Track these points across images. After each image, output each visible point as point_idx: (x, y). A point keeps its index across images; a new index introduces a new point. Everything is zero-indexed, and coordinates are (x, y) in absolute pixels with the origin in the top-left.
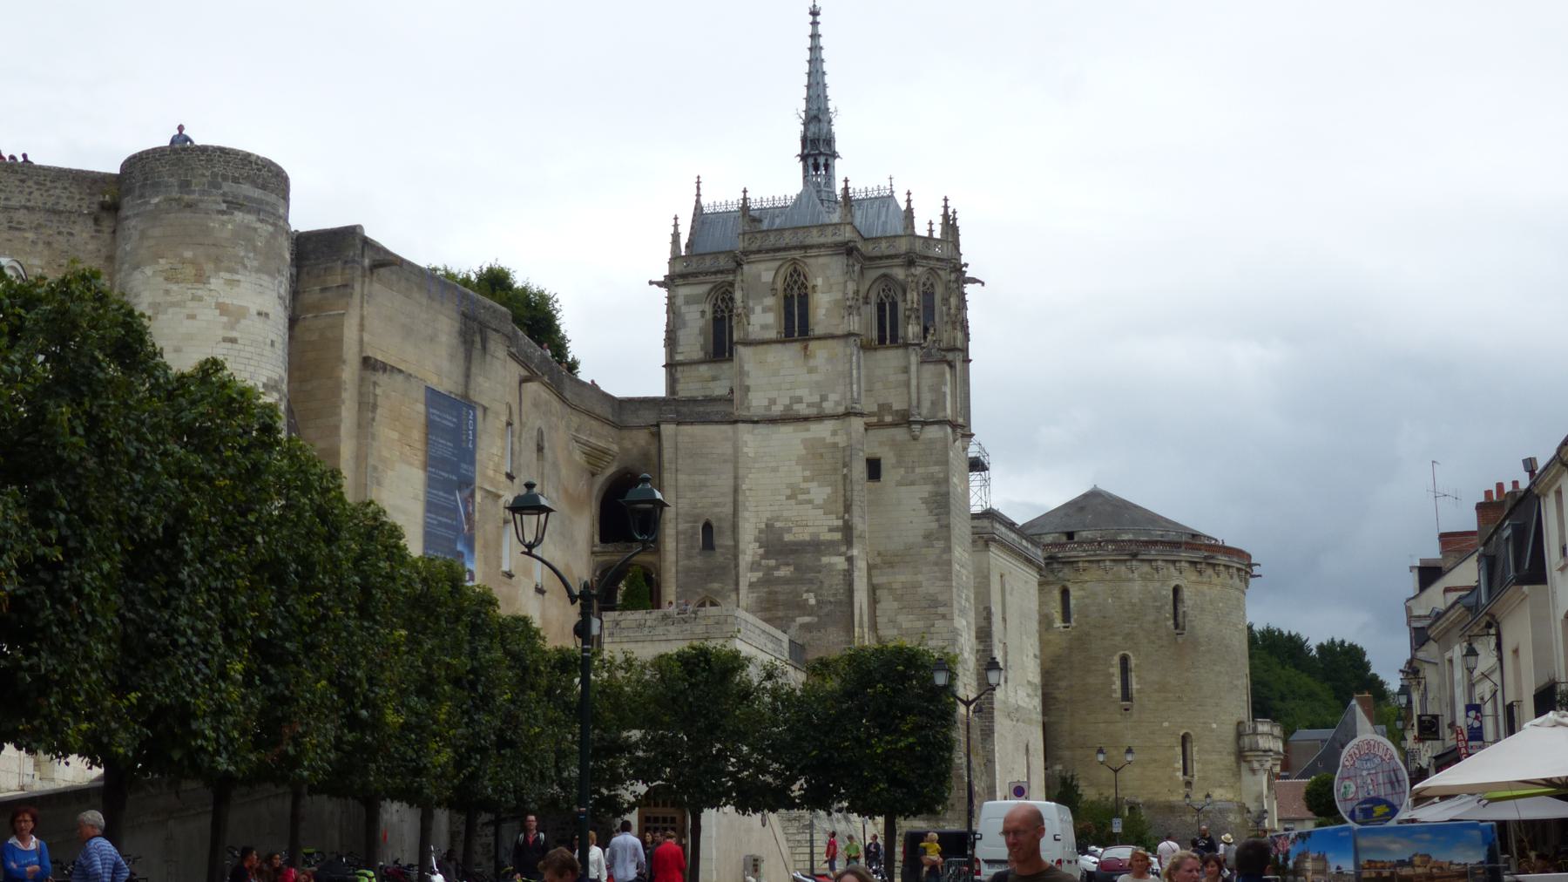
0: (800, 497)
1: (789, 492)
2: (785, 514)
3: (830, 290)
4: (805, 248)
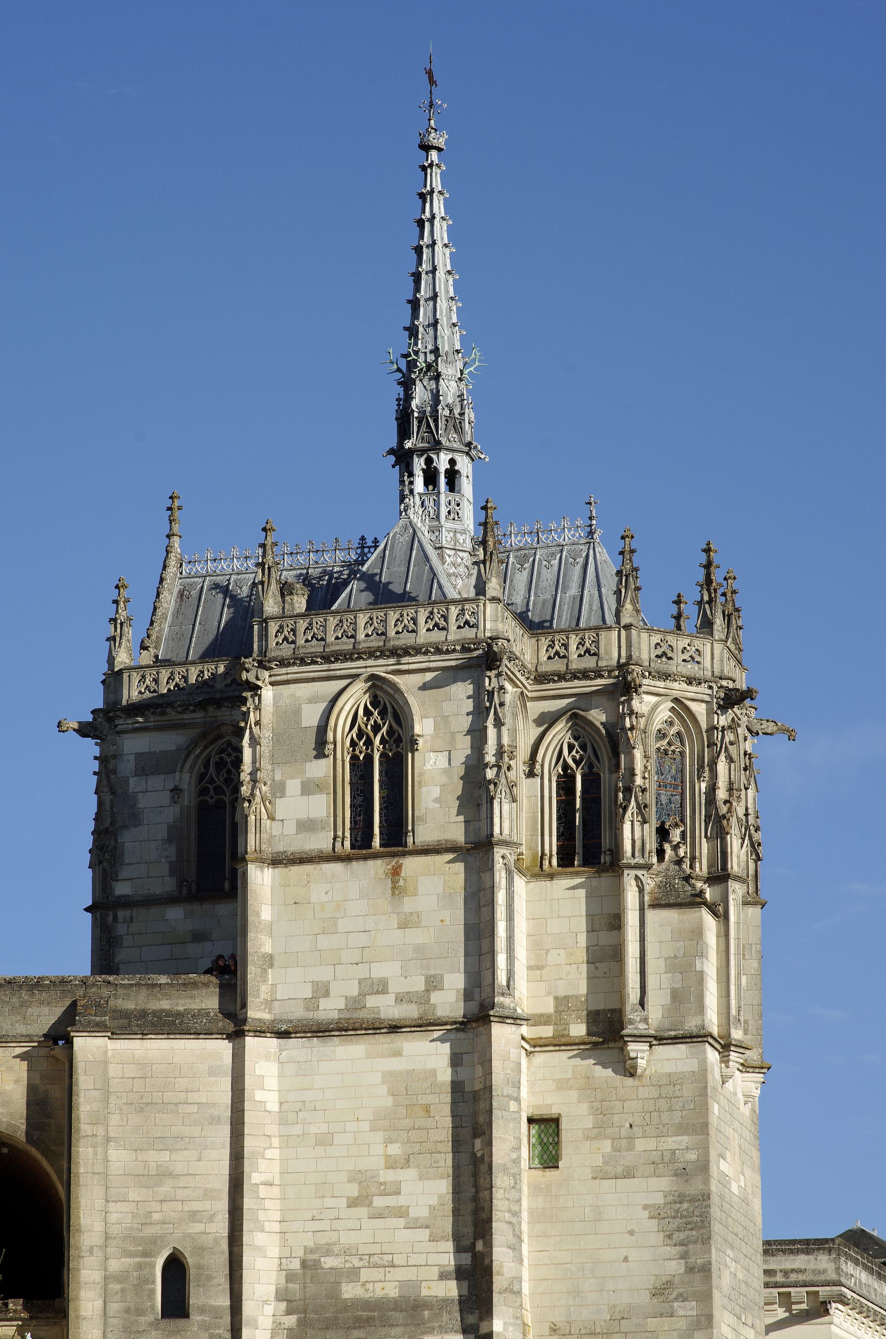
0: (379, 1202)
1: (353, 1190)
2: (347, 1239)
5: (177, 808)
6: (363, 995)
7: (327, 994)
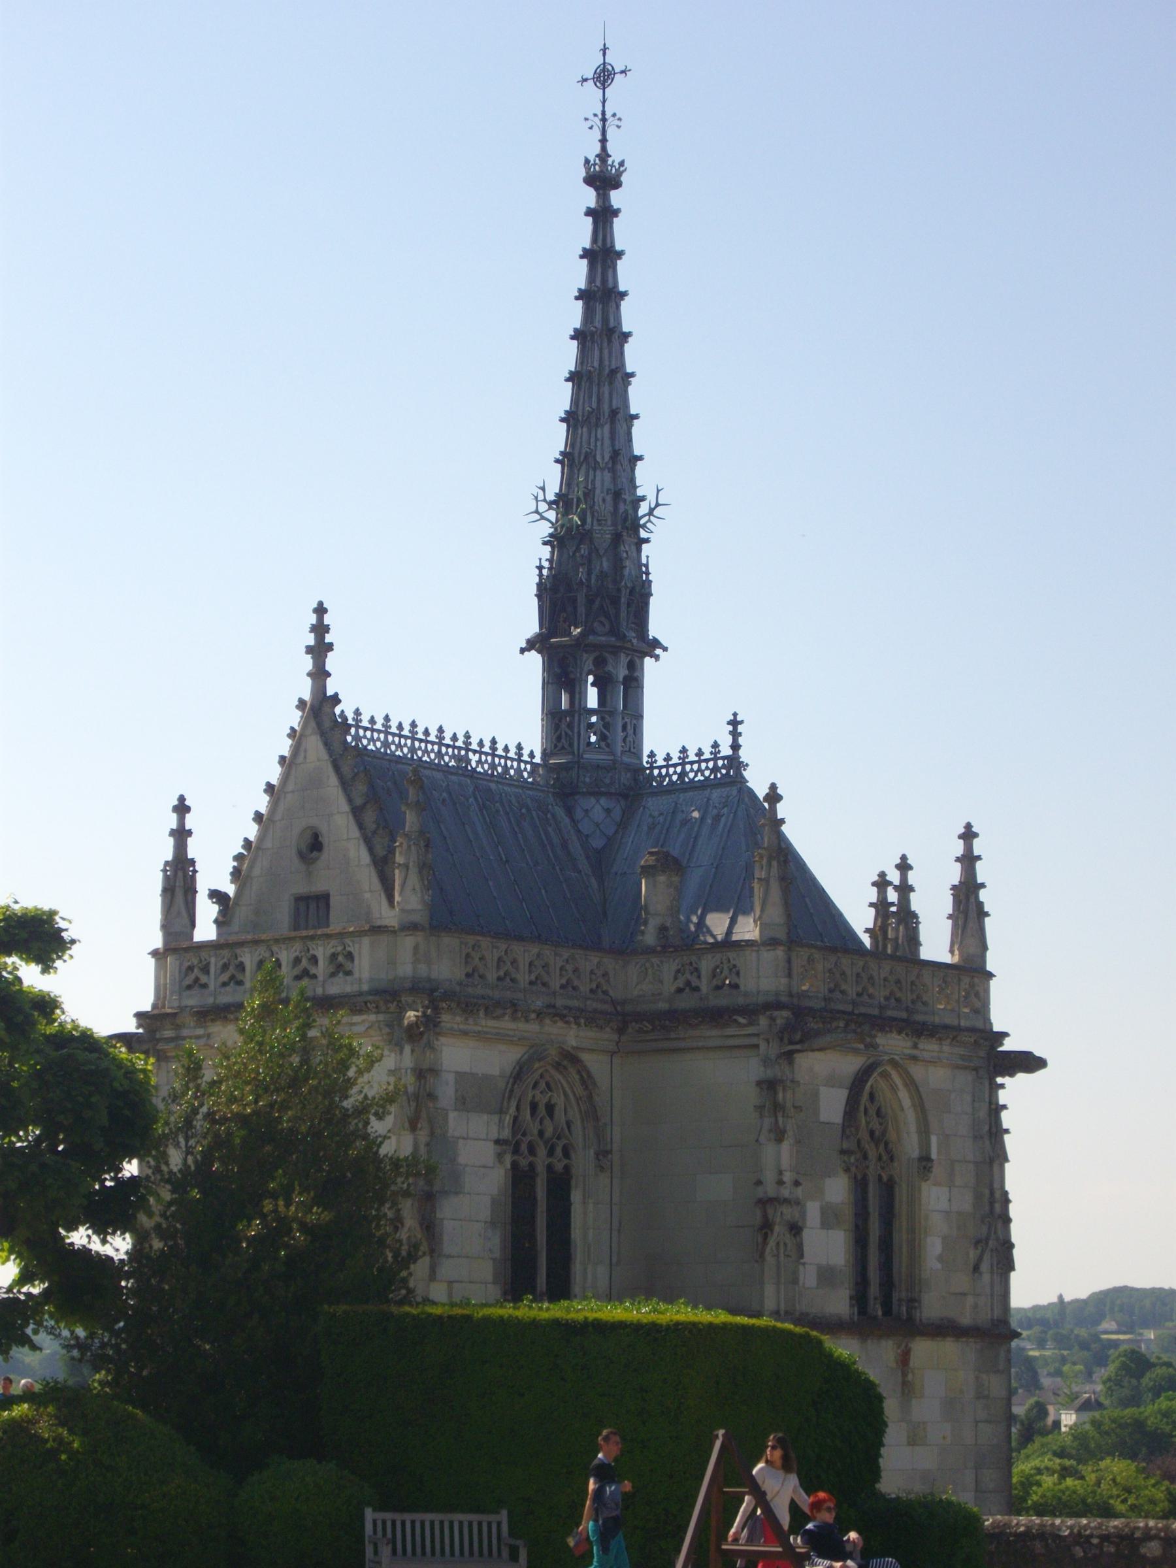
5: (502, 1172)
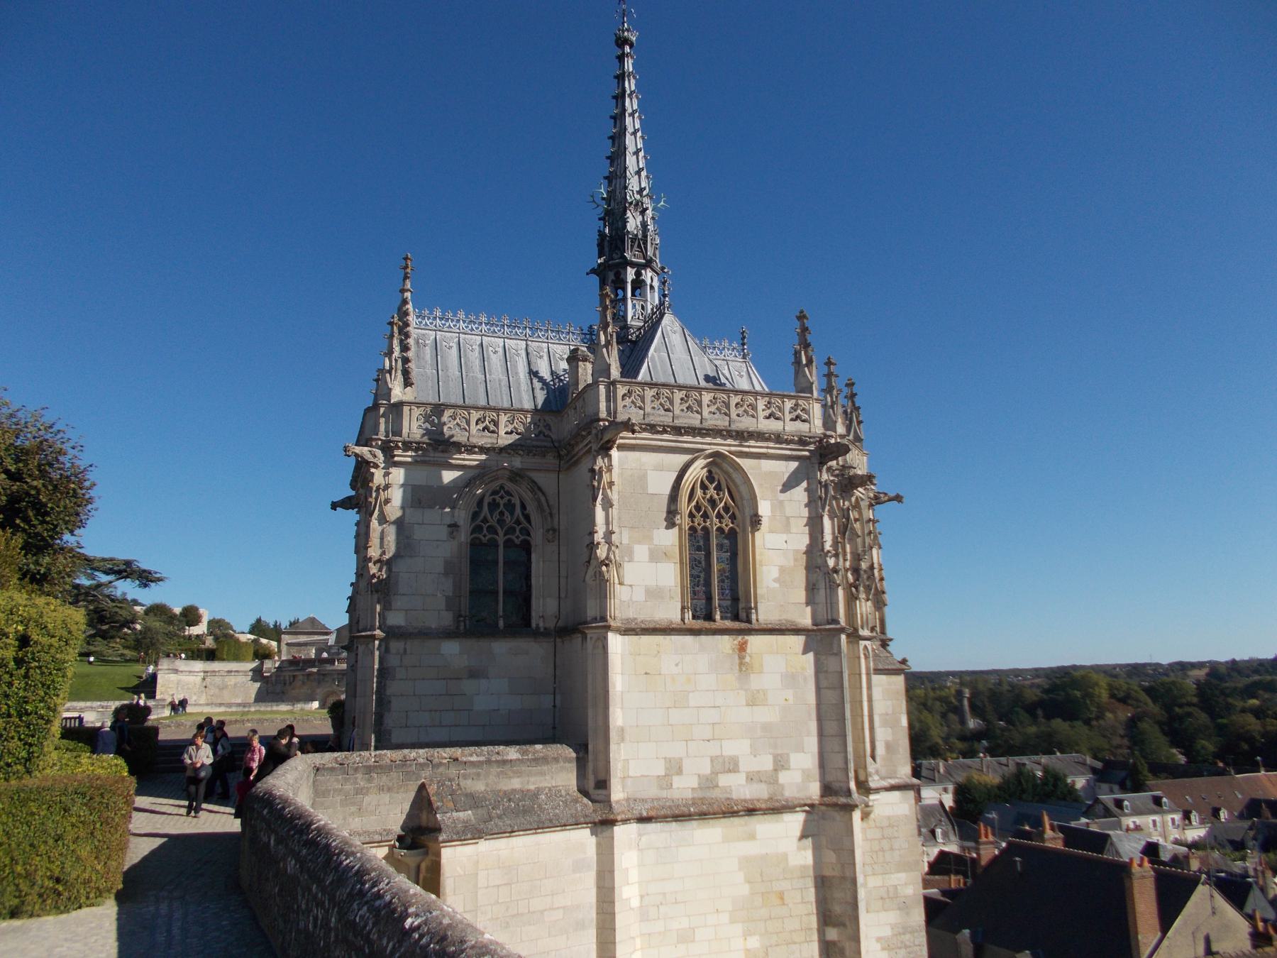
3: (787, 528)
4: (742, 436)
6: (715, 773)
7: (680, 772)
